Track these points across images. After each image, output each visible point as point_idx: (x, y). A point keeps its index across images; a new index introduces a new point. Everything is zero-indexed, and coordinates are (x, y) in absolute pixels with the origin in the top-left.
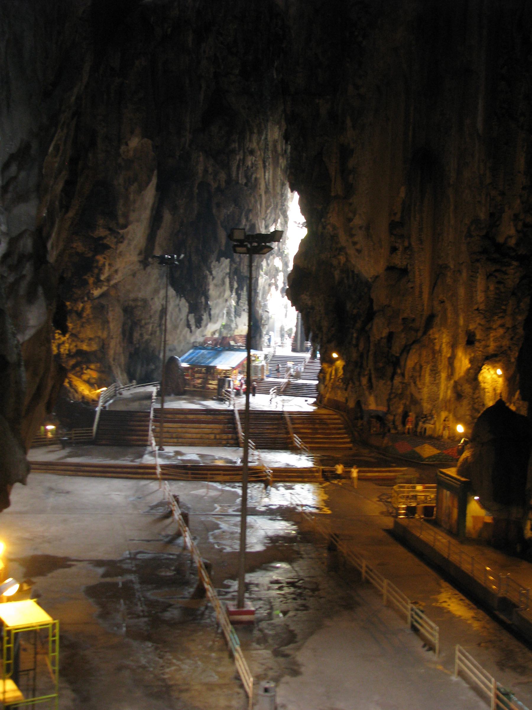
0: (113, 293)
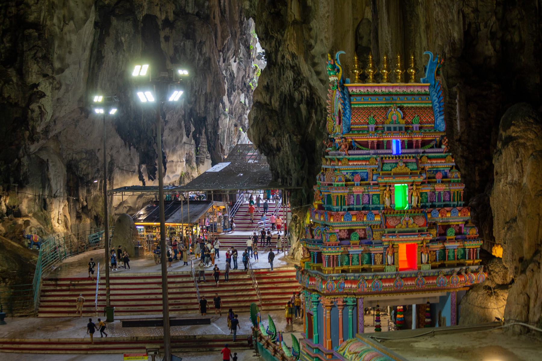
0: (52, 145)
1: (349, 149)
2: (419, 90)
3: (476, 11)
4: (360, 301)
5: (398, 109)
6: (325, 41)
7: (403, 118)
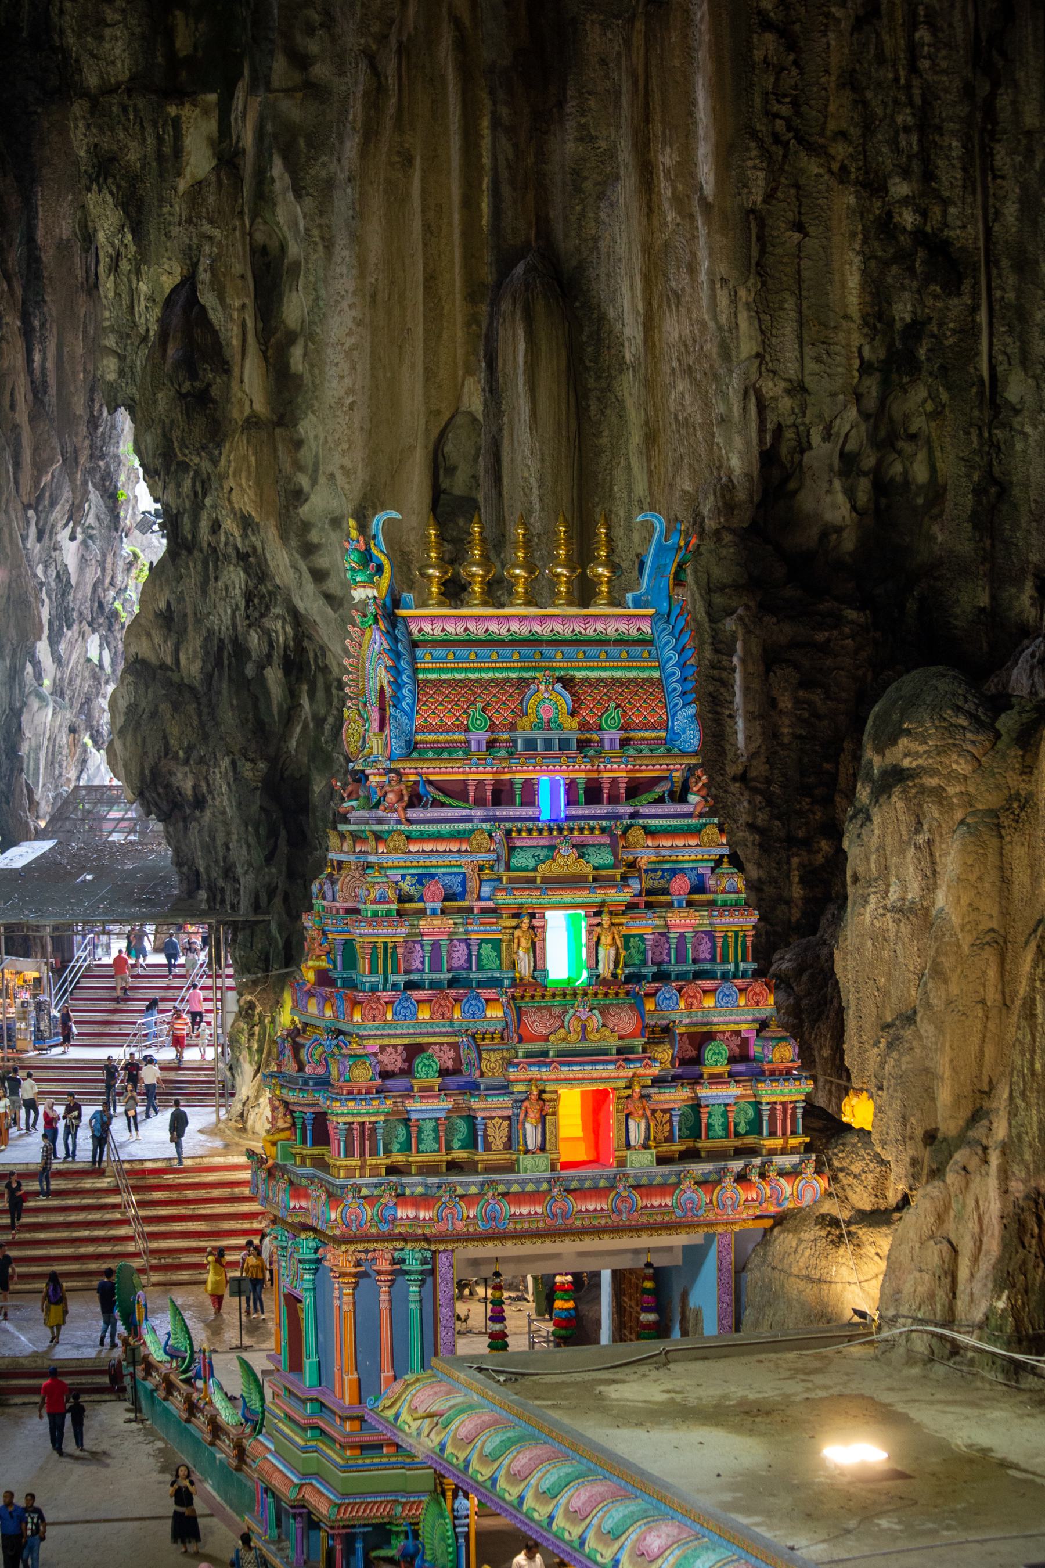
1: (411, 805)
2: (623, 627)
3: (798, 389)
4: (442, 1260)
5: (558, 686)
6: (340, 478)
7: (573, 713)
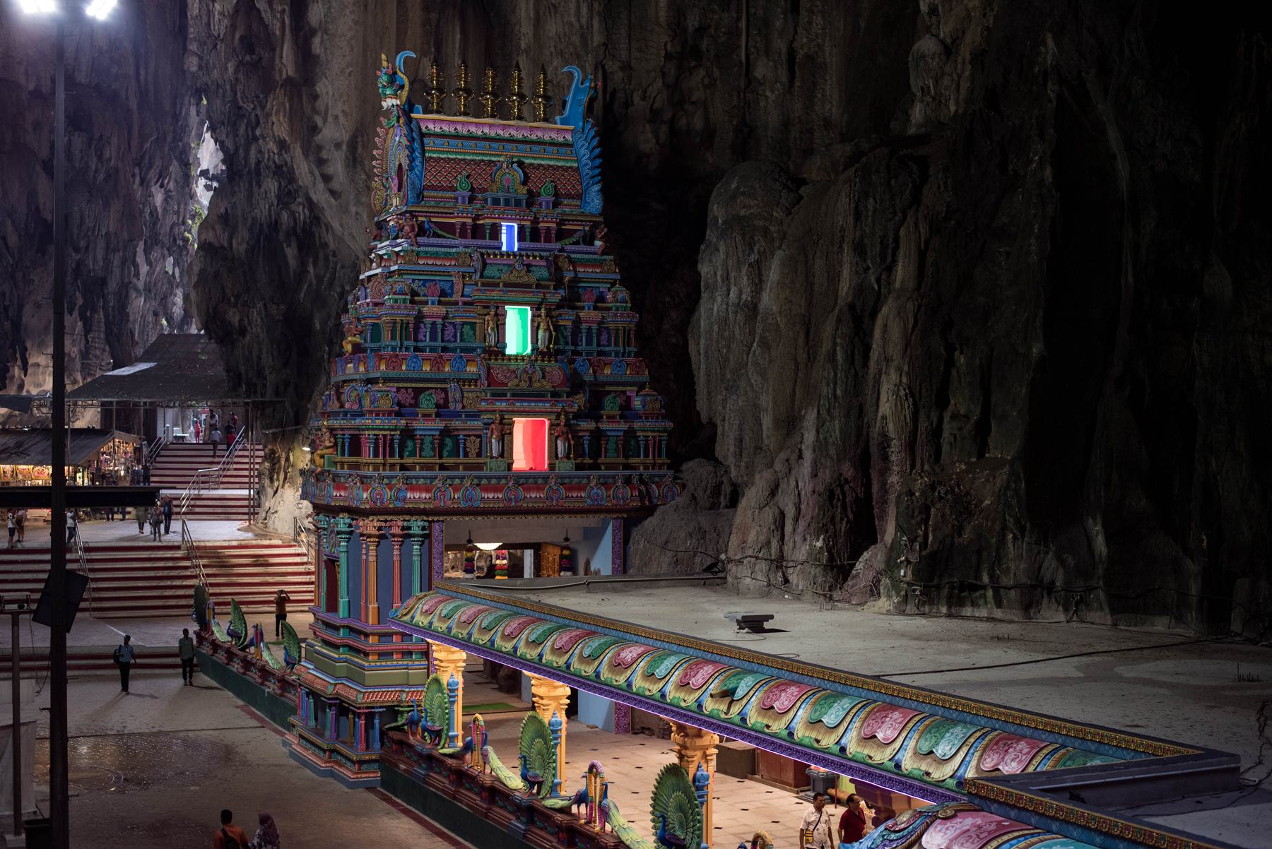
1: (418, 235)
2: (554, 136)
3: (627, 67)
4: (436, 526)
5: (515, 165)
6: (342, 119)
7: (524, 183)
